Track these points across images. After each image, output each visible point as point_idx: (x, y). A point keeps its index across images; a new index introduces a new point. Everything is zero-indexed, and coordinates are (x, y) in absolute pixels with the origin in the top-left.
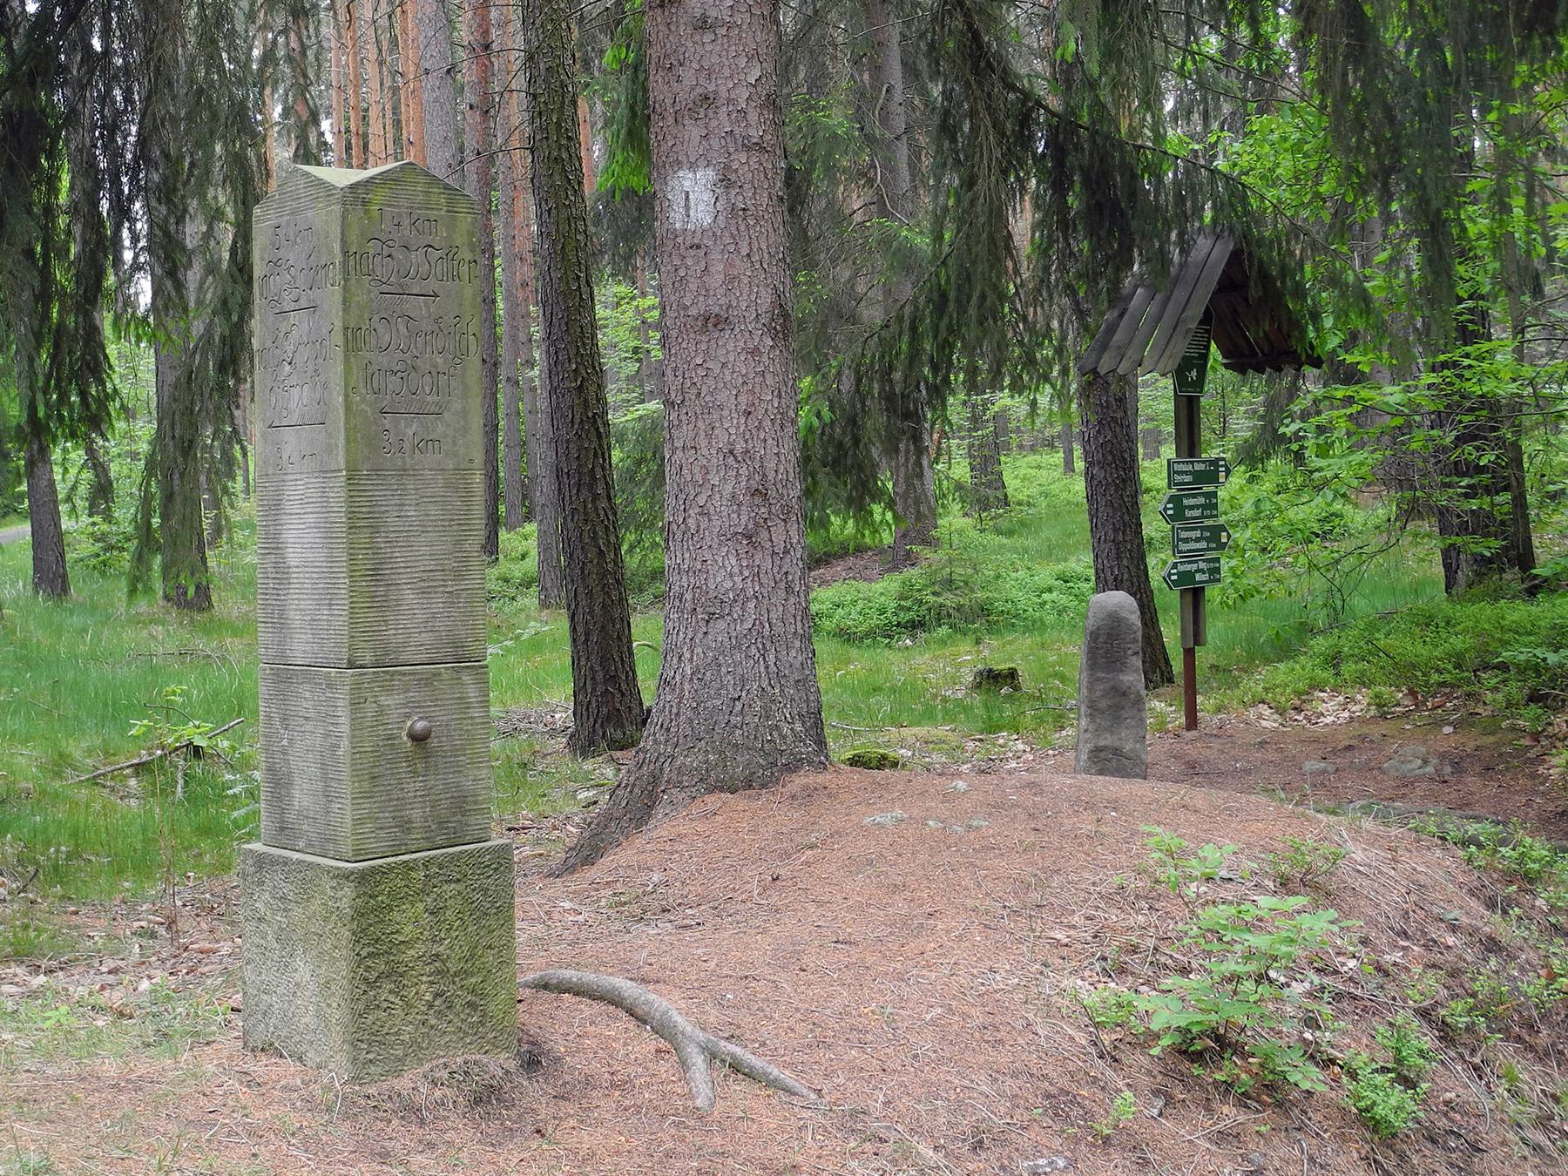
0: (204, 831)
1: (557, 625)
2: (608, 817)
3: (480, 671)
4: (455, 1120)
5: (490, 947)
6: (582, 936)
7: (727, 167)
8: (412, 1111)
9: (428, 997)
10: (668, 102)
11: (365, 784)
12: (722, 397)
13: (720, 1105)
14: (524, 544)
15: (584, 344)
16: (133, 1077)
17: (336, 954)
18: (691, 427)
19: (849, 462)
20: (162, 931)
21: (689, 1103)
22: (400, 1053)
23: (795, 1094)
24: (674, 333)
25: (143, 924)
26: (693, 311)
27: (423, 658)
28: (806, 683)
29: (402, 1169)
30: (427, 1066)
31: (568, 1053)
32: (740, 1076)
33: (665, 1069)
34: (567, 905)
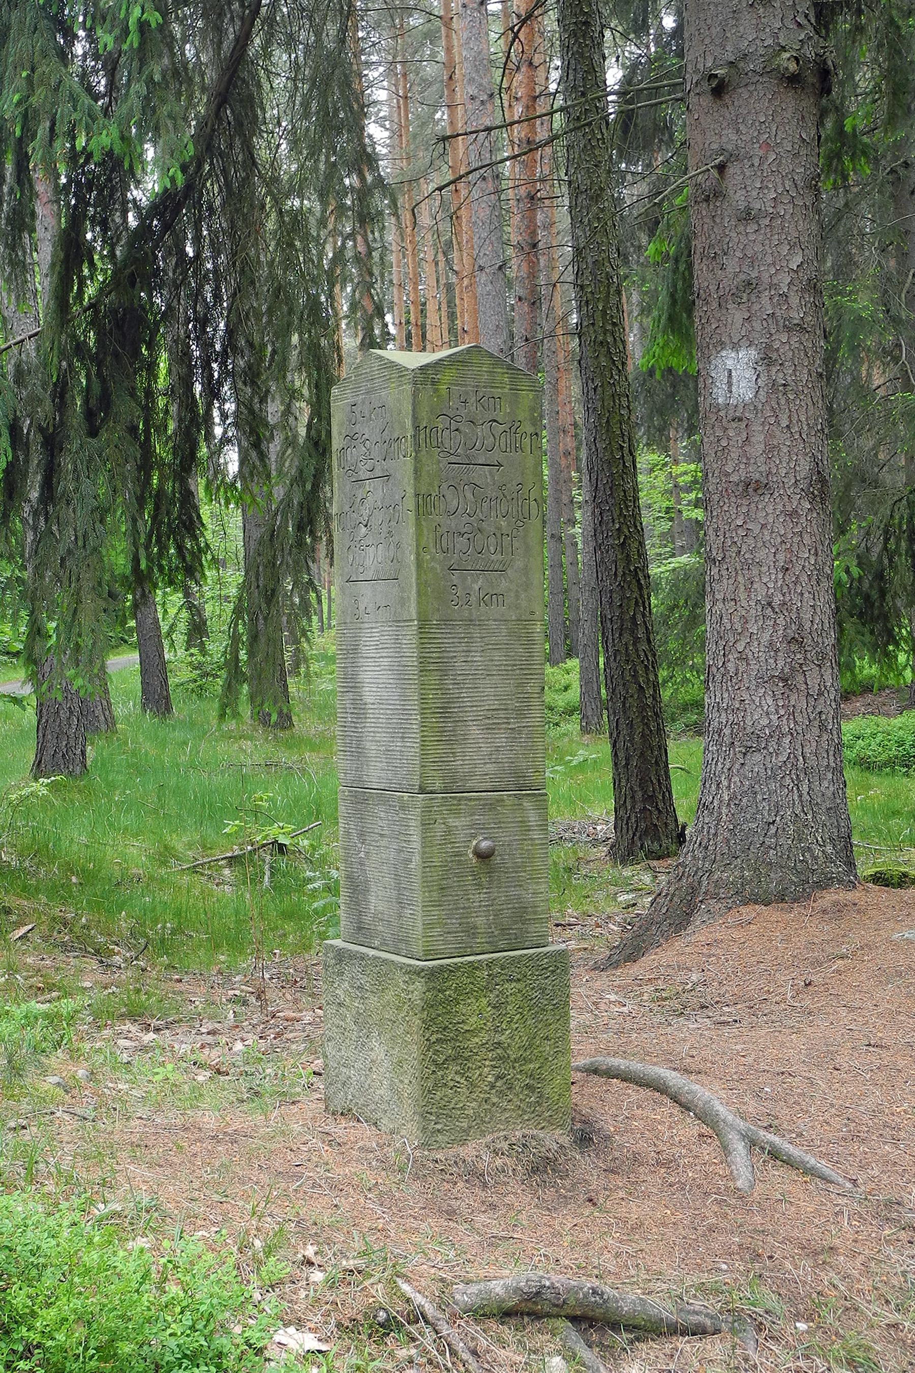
0: (287, 915)
1: (598, 750)
2: (649, 922)
3: (541, 801)
4: (514, 1185)
5: (547, 1038)
6: (628, 1026)
7: (768, 347)
8: (475, 1176)
9: (490, 1079)
10: (713, 288)
11: (435, 894)
12: (761, 555)
13: (759, 1188)
14: (567, 679)
15: (627, 507)
16: (229, 1130)
17: (408, 1038)
18: (731, 581)
19: (876, 612)
20: (252, 999)
21: (731, 1184)
22: (465, 1125)
23: (831, 1182)
24: (716, 497)
25: (237, 992)
26: (734, 478)
27: (488, 786)
28: (838, 809)
29: (467, 1226)
30: (489, 1138)
31: (617, 1132)
32: (779, 1163)
33: (708, 1151)
34: (613, 997)
